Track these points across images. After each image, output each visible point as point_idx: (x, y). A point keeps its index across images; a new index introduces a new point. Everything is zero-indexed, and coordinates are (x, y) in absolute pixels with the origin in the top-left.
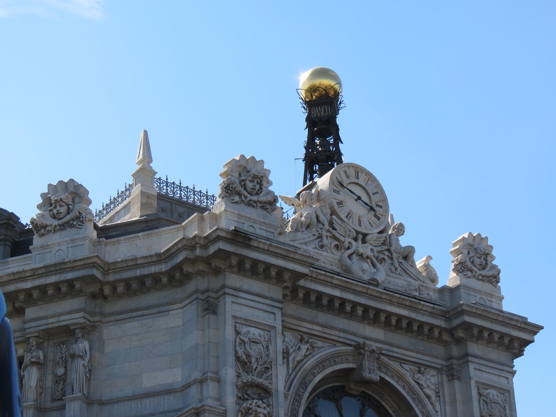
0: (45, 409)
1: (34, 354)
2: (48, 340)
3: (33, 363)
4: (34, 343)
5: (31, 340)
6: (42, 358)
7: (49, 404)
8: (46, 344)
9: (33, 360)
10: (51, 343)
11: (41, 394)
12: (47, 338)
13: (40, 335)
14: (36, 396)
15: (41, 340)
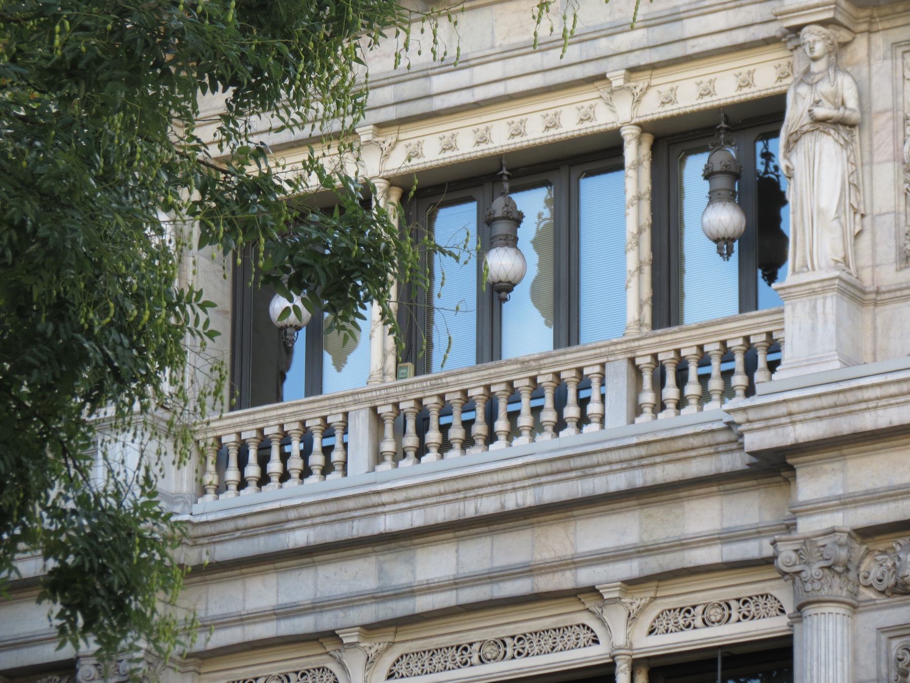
0: (878, 292)
1: (824, 87)
2: (870, 32)
3: (821, 123)
4: (819, 48)
5: (808, 35)
6: (852, 103)
7: (890, 275)
8: (860, 47)
9: (820, 112)
10: (880, 41)
11: (858, 235)
12: (864, 27)
13: (840, 18)
14: (839, 246)
15: (844, 36)
